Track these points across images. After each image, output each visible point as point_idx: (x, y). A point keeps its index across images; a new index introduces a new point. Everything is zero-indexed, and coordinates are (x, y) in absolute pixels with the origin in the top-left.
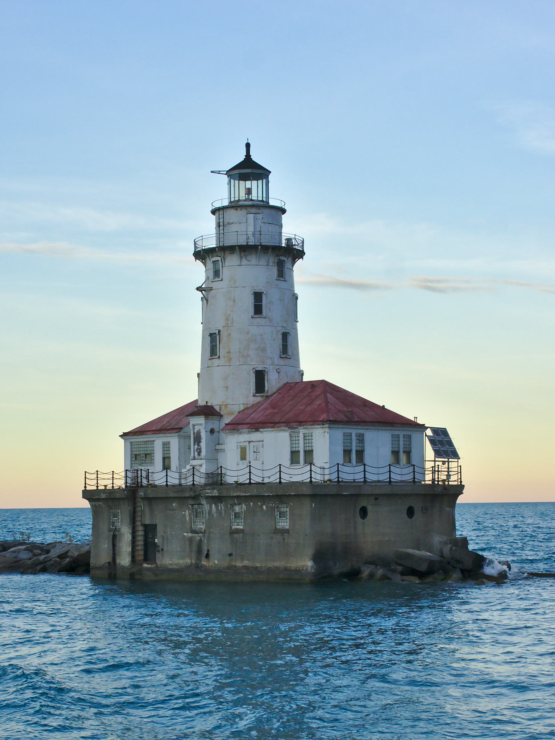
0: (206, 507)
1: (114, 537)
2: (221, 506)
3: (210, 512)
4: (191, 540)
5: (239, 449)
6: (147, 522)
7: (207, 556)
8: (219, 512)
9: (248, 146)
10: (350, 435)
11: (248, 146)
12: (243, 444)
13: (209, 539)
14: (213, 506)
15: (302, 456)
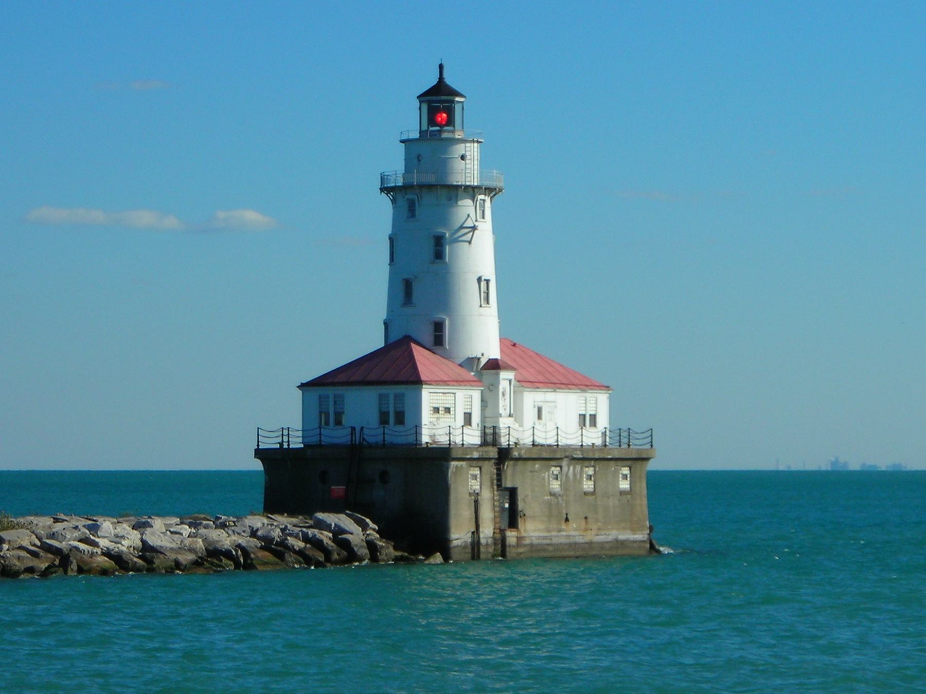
0: (565, 469)
1: (476, 502)
2: (578, 468)
3: (567, 475)
4: (549, 504)
5: (536, 409)
6: (509, 485)
7: (567, 520)
8: (575, 475)
9: (441, 67)
10: (387, 396)
11: (441, 67)
12: (540, 404)
13: (567, 503)
14: (571, 468)
15: (587, 420)
